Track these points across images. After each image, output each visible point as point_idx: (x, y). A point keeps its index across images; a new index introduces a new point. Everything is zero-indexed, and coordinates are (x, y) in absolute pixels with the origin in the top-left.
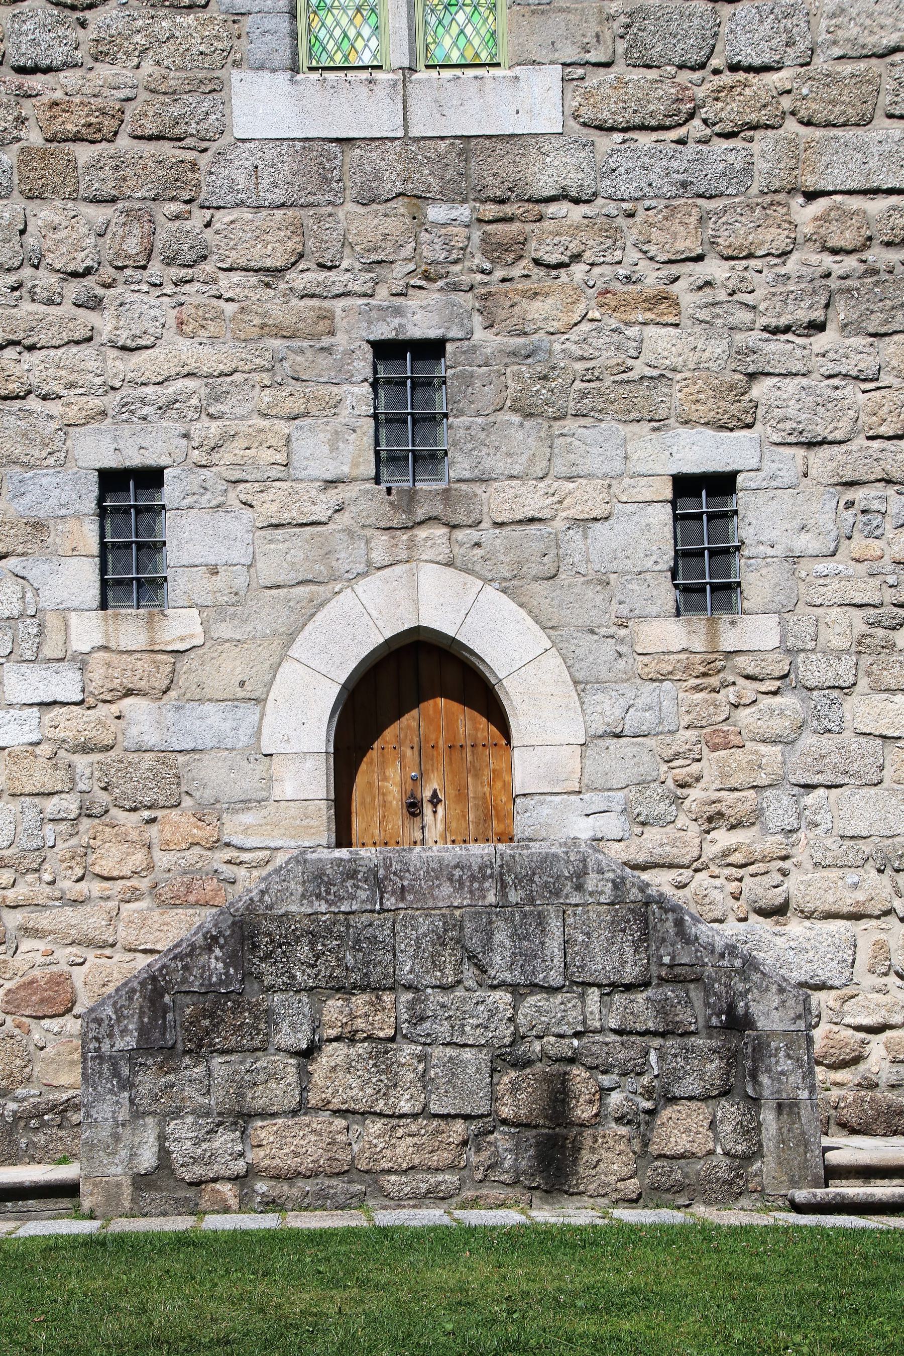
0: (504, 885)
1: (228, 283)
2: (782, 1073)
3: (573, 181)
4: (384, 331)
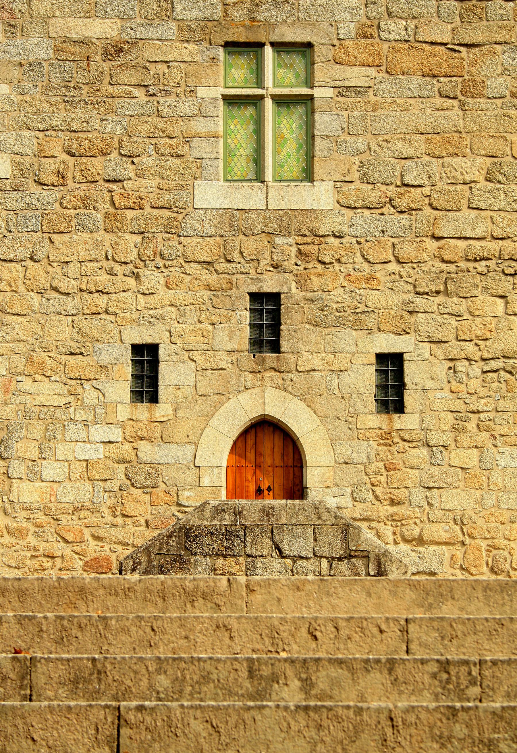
1: (191, 268)
4: (254, 289)
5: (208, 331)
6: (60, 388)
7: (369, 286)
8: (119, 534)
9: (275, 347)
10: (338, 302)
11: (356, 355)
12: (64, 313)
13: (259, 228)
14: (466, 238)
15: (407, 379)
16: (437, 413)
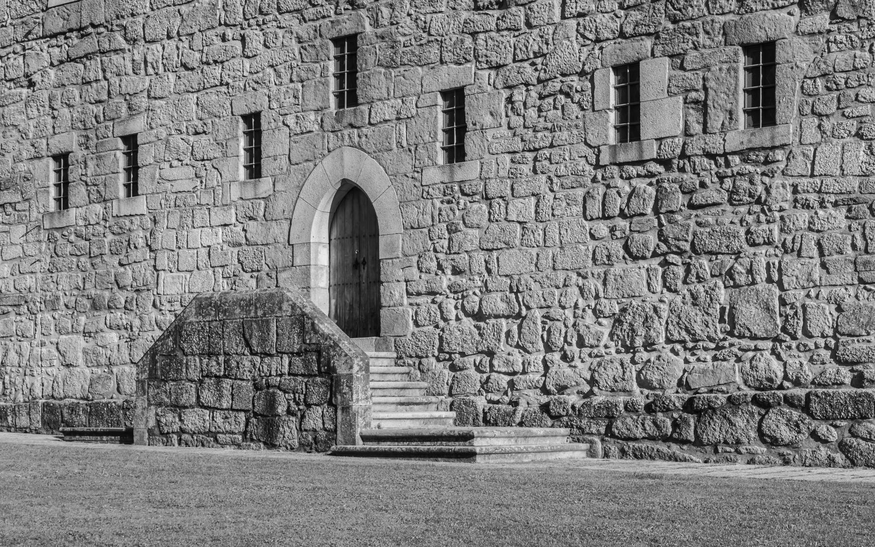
0: (256, 308)
5: (298, 91)
6: (191, 172)
7: (432, 8)
10: (405, 35)
11: (422, 96)
12: (191, 90)
16: (496, 156)
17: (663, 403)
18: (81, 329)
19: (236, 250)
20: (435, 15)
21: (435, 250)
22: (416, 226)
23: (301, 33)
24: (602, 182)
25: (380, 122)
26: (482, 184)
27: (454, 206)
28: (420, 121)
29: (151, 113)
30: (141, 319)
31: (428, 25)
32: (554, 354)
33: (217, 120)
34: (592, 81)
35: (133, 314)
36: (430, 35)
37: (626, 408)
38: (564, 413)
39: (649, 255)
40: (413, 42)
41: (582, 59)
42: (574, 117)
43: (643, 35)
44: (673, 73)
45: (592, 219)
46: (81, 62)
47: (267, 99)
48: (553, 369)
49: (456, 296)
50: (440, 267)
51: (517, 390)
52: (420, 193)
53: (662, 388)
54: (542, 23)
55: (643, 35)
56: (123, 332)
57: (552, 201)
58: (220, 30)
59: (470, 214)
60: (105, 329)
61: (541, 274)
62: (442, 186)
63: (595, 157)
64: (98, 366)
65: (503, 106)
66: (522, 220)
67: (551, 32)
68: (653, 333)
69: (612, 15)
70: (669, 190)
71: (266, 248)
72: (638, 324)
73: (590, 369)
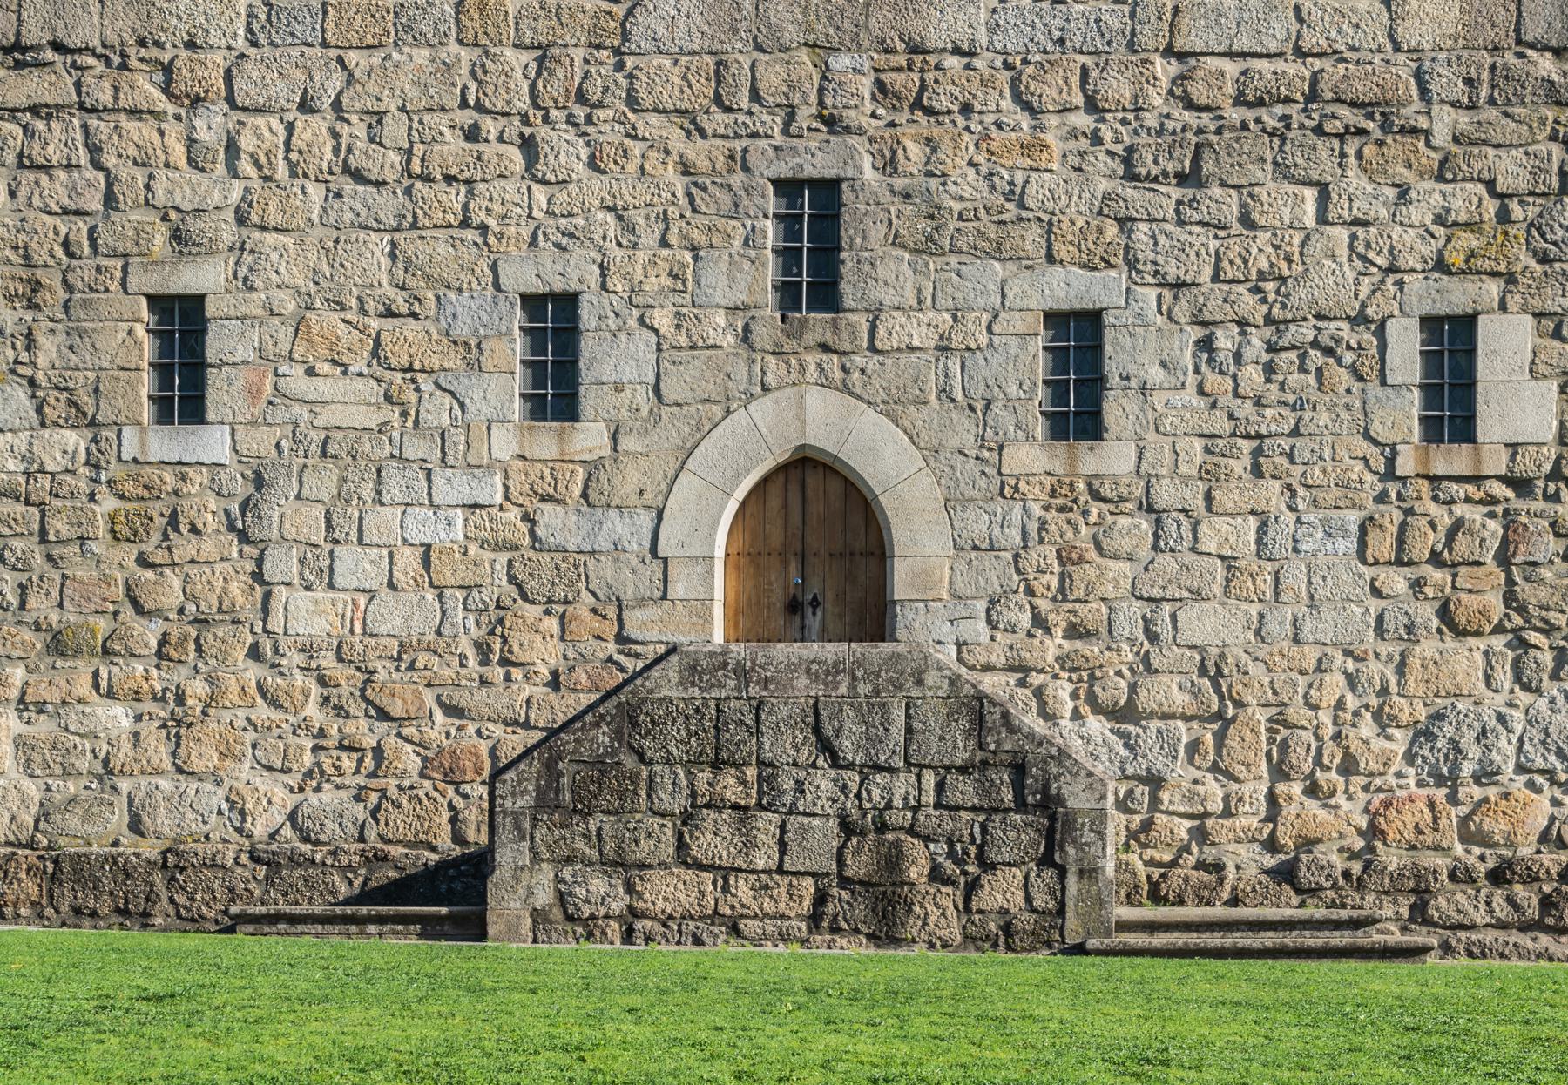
0: (854, 678)
2: (1086, 844)
3: (962, 35)
4: (784, 171)
5: (683, 266)
7: (1029, 161)
8: (497, 700)
9: (827, 296)
10: (962, 199)
11: (1003, 315)
12: (375, 225)
13: (791, 34)
14: (1243, 55)
15: (1112, 369)
16: (1171, 439)
17: (1529, 868)
18: (14, 693)
19: (503, 558)
20: (1034, 175)
21: (1030, 592)
22: (986, 545)
23: (691, 155)
24: (1397, 503)
25: (899, 350)
26: (1142, 483)
27: (1076, 516)
28: (997, 359)
29: (248, 259)
30: (210, 680)
31: (1018, 190)
32: (1293, 784)
33: (452, 295)
34: (1380, 332)
35: (184, 671)
36: (1022, 205)
37: (1452, 876)
38: (1328, 885)
39: (1488, 629)
40: (982, 213)
41: (1362, 296)
42: (1342, 390)
43: (1486, 273)
44: (1539, 341)
45: (1376, 563)
46: (15, 120)
47: (598, 271)
48: (1289, 811)
49: (1075, 676)
50: (1039, 621)
51: (1213, 844)
52: (995, 488)
53: (1512, 845)
54: (1278, 224)
55: (1486, 273)
56: (148, 706)
57: (1292, 527)
58: (467, 117)
59: (1115, 534)
60: (94, 697)
61: (1268, 649)
62: (1048, 481)
63: (1383, 460)
64: (66, 774)
65: (1189, 353)
66: (1227, 552)
67: (1297, 241)
68: (1494, 755)
69: (1421, 231)
70: (1531, 528)
71: (591, 562)
72: (1467, 740)
73: (1366, 811)
